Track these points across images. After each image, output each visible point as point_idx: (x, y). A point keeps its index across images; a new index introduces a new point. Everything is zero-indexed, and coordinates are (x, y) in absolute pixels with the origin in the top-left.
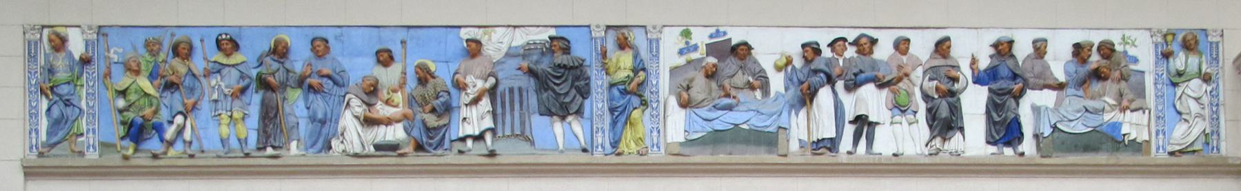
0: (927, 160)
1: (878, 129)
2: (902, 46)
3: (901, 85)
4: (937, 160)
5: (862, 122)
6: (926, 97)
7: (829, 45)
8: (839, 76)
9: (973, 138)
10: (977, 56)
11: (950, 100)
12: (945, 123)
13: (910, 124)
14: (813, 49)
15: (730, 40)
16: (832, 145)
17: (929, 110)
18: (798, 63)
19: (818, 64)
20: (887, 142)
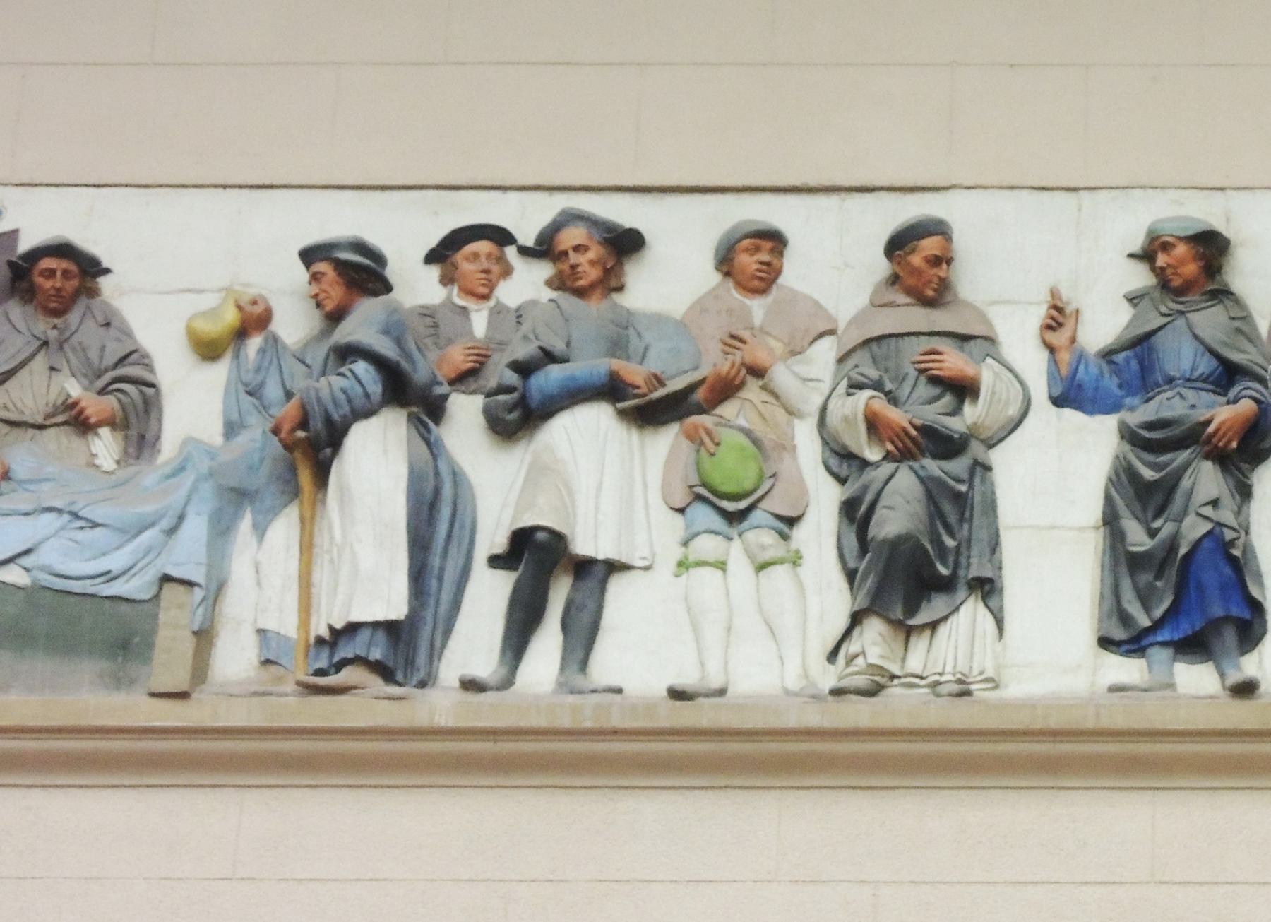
0: (814, 718)
1: (621, 597)
2: (753, 258)
3: (728, 410)
4: (859, 713)
5: (536, 556)
6: (843, 461)
7: (433, 257)
8: (463, 379)
9: (1043, 625)
10: (1072, 297)
11: (933, 467)
12: (919, 568)
13: (762, 567)
14: (343, 267)
15: (13, 235)
16: (400, 650)
17: (849, 508)
18: (294, 323)
19: (364, 324)
20: (646, 645)
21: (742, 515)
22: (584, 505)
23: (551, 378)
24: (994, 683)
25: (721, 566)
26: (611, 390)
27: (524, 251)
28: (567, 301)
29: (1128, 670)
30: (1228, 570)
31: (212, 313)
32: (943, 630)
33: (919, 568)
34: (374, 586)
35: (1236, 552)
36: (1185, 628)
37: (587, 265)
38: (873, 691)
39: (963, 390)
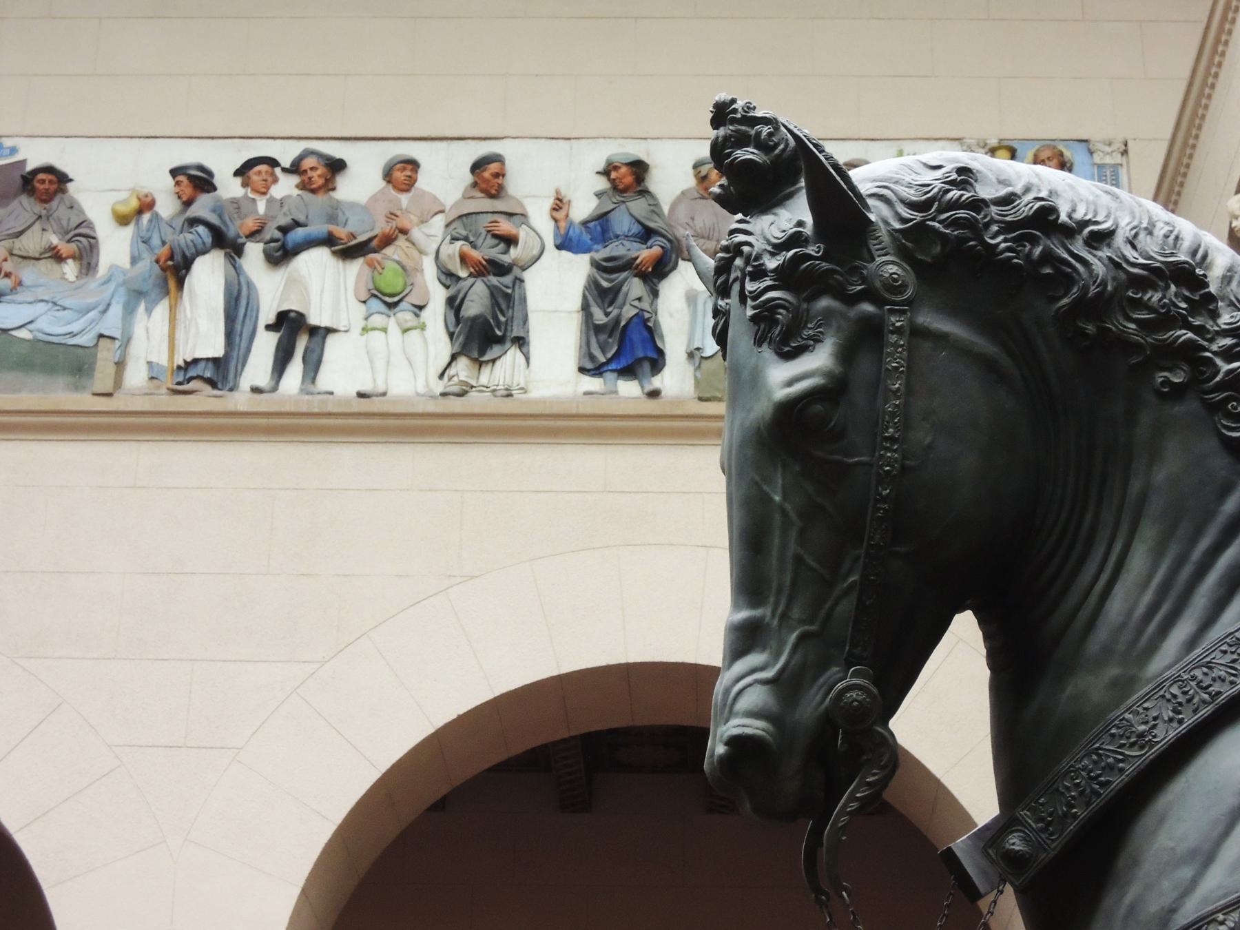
0: (431, 407)
1: (334, 348)
2: (402, 174)
3: (389, 251)
4: (455, 405)
5: (290, 325)
6: (448, 277)
7: (239, 173)
8: (253, 235)
10: (566, 193)
11: (494, 280)
12: (486, 332)
13: (405, 331)
14: (192, 178)
15: (23, 162)
16: (220, 372)
17: (450, 301)
18: (167, 207)
20: (345, 370)
21: (396, 304)
22: (315, 299)
23: (298, 234)
24: (524, 390)
25: (385, 330)
26: (329, 241)
27: (284, 170)
28: (307, 196)
29: (593, 384)
30: (646, 334)
31: (125, 202)
32: (498, 363)
33: (486, 332)
34: (208, 341)
35: (650, 324)
36: (623, 363)
37: (317, 177)
38: (462, 394)
39: (509, 241)
